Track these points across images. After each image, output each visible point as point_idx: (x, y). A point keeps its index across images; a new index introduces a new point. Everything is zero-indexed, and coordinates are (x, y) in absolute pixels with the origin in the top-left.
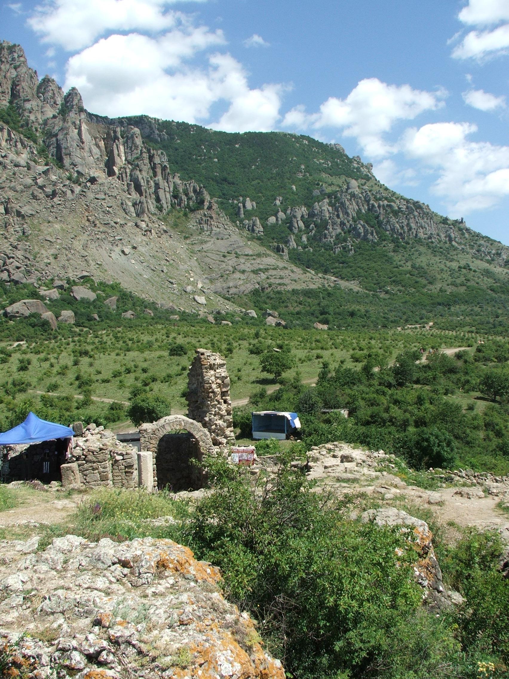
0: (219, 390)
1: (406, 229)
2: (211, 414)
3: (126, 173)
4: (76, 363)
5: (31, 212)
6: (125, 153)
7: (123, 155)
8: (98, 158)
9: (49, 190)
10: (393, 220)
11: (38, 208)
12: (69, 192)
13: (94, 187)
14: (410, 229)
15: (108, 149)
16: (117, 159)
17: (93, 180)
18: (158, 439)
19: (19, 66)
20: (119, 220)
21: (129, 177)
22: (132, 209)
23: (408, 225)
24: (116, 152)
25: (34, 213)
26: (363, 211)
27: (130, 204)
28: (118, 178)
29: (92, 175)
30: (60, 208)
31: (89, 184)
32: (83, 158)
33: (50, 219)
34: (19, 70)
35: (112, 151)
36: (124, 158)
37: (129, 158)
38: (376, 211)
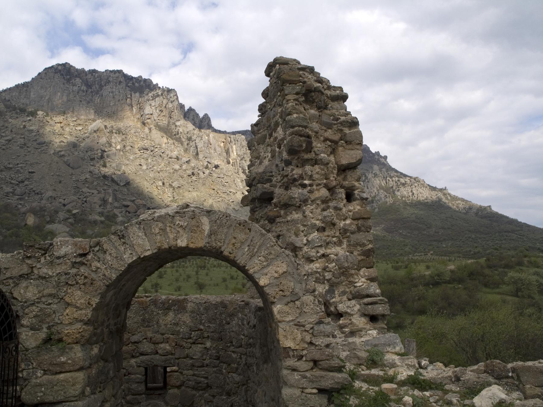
0: (332, 158)
1: (410, 194)
2: (314, 226)
3: (237, 162)
4: (197, 273)
5: (178, 185)
6: (236, 150)
7: (235, 151)
8: (220, 154)
9: (189, 172)
10: (402, 189)
11: (183, 183)
12: (201, 174)
13: (217, 170)
14: (413, 194)
15: (226, 149)
16: (232, 154)
17: (217, 167)
18: (100, 285)
19: (174, 101)
20: (232, 190)
21: (238, 165)
22: (240, 184)
23: (412, 191)
24: (230, 150)
25: (180, 186)
26: (383, 184)
27: (239, 180)
28: (232, 165)
29: (216, 164)
30: (196, 183)
31: (214, 169)
32: (210, 153)
33: (190, 189)
34: (173, 103)
35: (228, 149)
36: (235, 154)
37: (239, 153)
38: (391, 184)
